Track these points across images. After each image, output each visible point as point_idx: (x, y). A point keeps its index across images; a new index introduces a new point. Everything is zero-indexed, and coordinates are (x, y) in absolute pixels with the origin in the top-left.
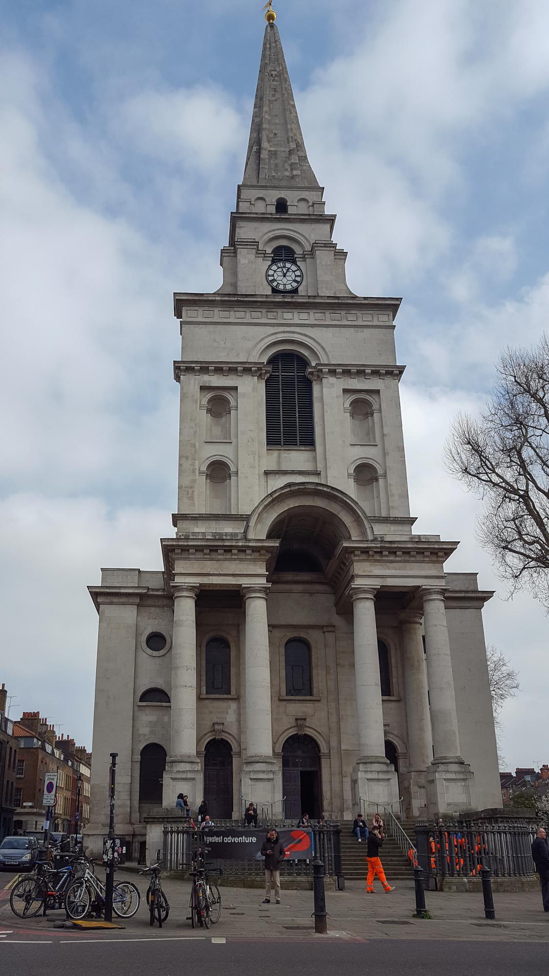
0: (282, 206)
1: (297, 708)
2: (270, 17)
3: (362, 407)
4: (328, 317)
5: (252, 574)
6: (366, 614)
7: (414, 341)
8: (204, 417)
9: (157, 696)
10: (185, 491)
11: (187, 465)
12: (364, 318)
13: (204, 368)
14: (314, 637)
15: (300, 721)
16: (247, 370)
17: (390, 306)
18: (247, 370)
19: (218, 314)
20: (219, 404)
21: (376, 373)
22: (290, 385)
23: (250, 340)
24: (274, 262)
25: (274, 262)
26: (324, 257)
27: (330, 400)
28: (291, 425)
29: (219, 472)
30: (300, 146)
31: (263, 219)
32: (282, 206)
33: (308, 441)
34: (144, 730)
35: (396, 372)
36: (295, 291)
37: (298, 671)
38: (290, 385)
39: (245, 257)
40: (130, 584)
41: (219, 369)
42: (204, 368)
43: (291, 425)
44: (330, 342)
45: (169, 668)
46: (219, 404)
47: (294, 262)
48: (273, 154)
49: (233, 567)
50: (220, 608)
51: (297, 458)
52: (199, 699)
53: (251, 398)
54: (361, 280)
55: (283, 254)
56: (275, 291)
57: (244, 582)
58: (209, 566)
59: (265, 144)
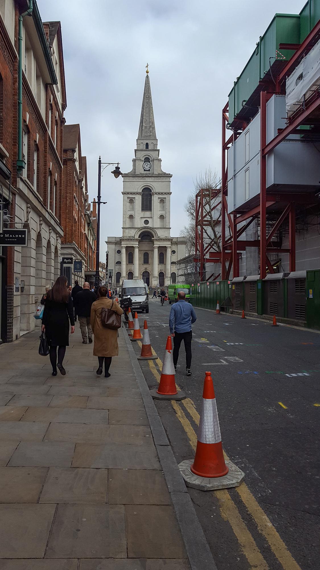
0: (147, 144)
1: (146, 266)
2: (147, 77)
3: (162, 201)
4: (156, 179)
5: (136, 244)
6: (156, 251)
7: (174, 187)
8: (128, 204)
9: (119, 263)
10: (124, 222)
11: (125, 216)
12: (164, 179)
13: (128, 193)
14: (149, 252)
15: (146, 269)
16: (137, 194)
17: (169, 176)
18: (138, 193)
19: (131, 179)
20: (131, 201)
21: (165, 194)
22: (147, 194)
23: (138, 186)
24: (145, 162)
25: (145, 162)
26: (156, 162)
27: (155, 199)
28: (147, 206)
29: (131, 217)
30: (153, 123)
31: (142, 150)
32: (147, 144)
33: (150, 210)
34: (117, 270)
35: (170, 193)
36: (149, 170)
37: (146, 259)
38: (147, 194)
39: (137, 162)
40: (113, 240)
41: (131, 194)
42: (128, 193)
43: (147, 206)
44: (156, 186)
45: (121, 258)
46: (131, 201)
47: (149, 162)
48: (146, 127)
49: (132, 243)
50: (130, 252)
51: (147, 214)
52: (127, 264)
53: (138, 199)
54: (165, 167)
55: (147, 160)
56: (145, 170)
57: (134, 246)
58: (128, 243)
59: (144, 124)
